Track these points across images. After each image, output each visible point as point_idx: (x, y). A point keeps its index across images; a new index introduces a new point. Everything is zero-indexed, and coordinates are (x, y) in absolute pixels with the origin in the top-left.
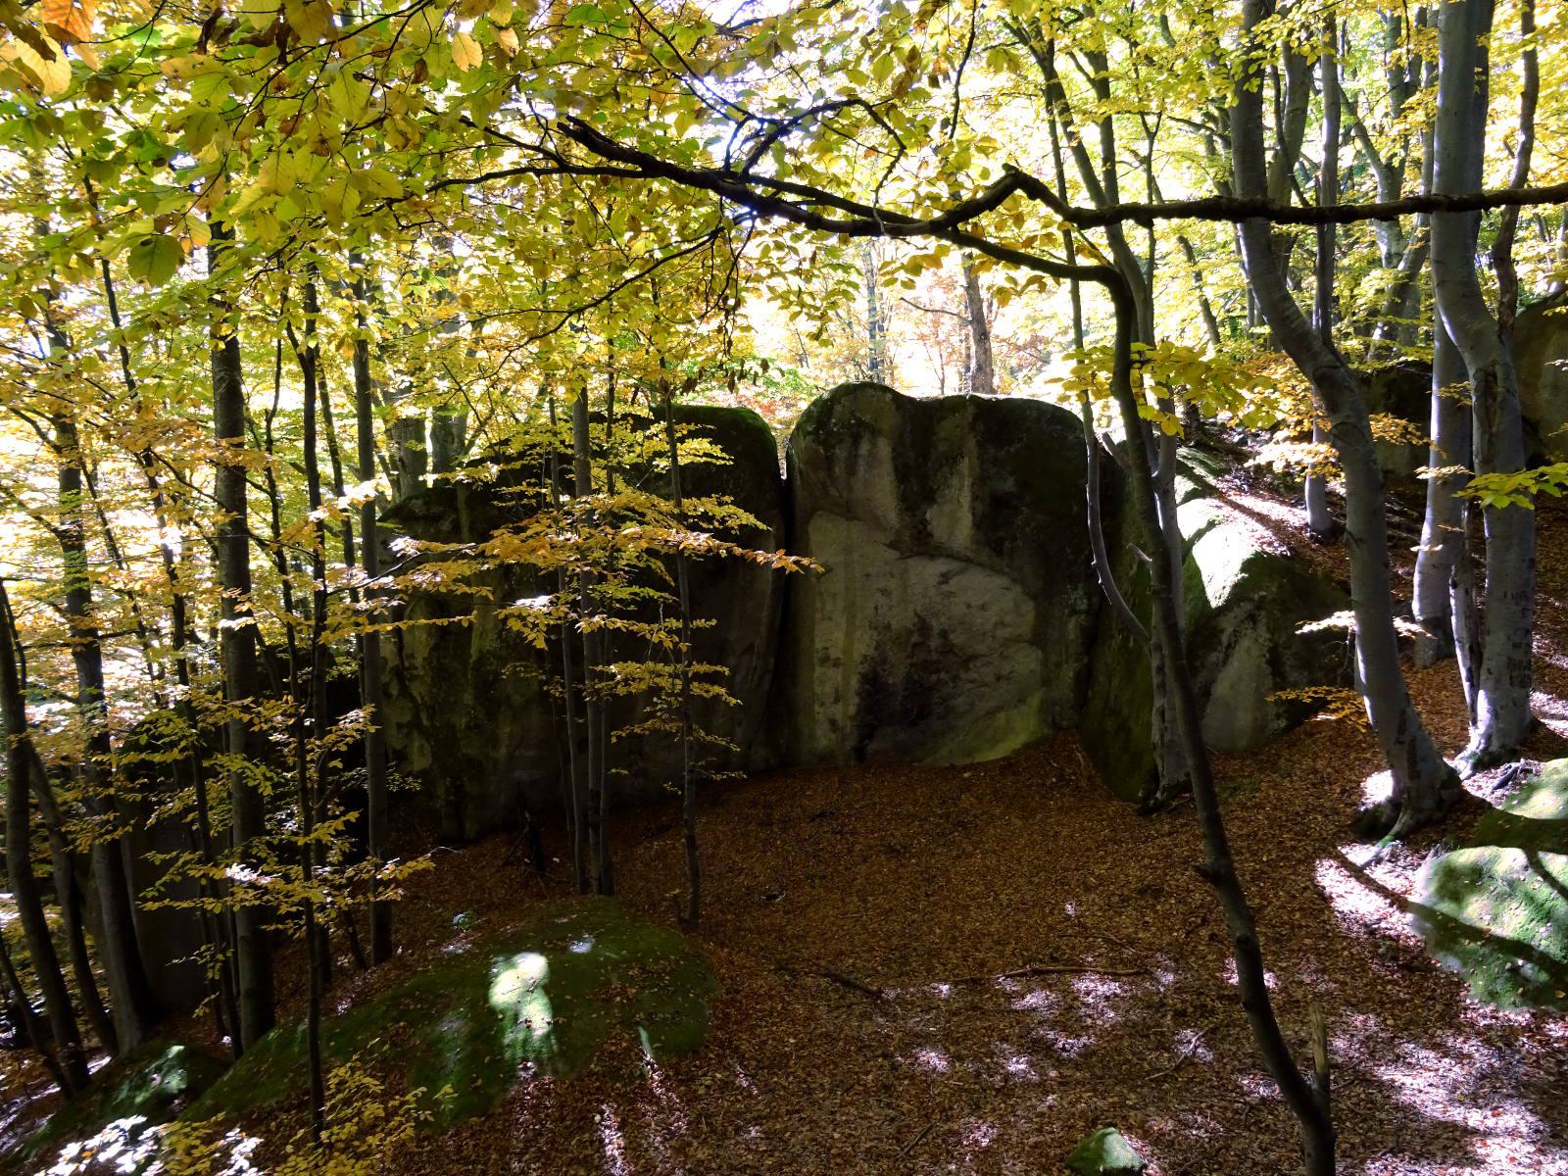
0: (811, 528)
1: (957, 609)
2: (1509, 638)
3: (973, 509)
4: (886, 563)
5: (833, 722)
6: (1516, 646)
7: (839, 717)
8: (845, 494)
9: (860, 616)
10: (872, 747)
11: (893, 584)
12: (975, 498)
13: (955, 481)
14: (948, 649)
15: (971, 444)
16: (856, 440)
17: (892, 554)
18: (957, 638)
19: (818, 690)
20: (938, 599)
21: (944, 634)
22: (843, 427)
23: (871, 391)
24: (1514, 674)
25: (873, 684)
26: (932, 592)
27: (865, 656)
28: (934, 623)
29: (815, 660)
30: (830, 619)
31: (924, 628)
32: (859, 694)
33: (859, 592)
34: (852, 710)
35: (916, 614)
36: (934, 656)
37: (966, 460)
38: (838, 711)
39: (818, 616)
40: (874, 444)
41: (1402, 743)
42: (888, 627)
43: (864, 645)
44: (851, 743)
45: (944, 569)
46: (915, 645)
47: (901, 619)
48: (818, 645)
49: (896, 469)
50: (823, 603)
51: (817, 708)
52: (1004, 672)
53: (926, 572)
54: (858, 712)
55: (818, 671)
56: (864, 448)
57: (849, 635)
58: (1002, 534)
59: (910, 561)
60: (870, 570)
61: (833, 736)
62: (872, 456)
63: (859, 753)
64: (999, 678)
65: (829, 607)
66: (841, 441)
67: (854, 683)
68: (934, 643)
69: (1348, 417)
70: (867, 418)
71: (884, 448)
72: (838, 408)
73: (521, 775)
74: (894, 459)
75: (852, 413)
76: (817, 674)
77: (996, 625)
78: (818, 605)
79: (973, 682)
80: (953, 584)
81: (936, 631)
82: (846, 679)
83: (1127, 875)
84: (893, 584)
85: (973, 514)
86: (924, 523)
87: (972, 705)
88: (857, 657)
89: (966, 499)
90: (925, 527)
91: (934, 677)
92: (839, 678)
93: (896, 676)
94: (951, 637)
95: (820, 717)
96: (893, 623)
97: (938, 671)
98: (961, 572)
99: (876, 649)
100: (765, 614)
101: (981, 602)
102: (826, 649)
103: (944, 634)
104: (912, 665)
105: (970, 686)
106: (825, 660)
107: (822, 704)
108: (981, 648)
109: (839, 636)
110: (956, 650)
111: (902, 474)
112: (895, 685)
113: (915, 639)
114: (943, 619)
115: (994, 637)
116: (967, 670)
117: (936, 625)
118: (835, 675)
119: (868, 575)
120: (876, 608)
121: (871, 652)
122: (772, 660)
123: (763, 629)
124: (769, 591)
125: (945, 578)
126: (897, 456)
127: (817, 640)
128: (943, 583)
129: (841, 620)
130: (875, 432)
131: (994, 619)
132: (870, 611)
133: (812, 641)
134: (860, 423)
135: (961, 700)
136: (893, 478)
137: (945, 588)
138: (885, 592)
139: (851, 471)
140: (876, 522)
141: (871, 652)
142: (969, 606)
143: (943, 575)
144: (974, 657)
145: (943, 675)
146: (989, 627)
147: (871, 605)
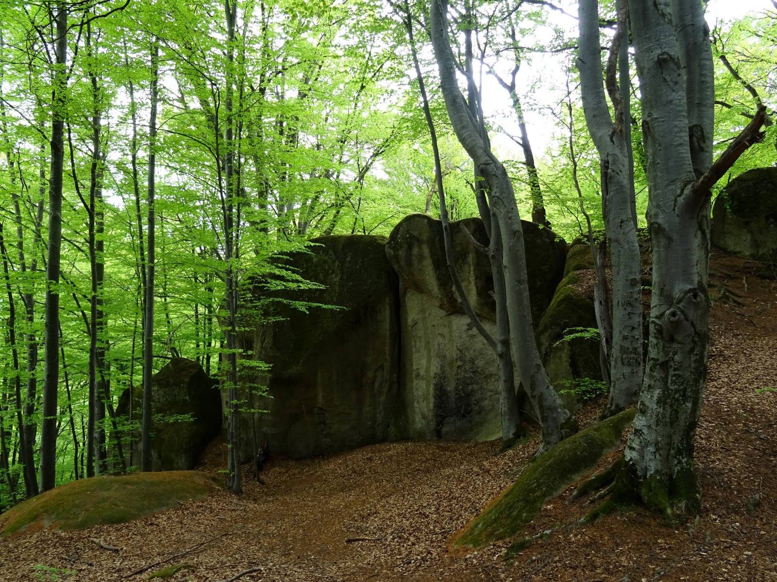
0: (406, 299)
3: (476, 284)
4: (441, 318)
9: (432, 351)
10: (445, 429)
11: (446, 331)
12: (477, 278)
13: (466, 267)
16: (410, 247)
17: (443, 313)
18: (480, 363)
19: (415, 394)
20: (467, 339)
21: (472, 361)
23: (418, 219)
24: (624, 356)
25: (441, 393)
26: (464, 335)
27: (436, 374)
28: (467, 354)
29: (414, 375)
30: (419, 352)
33: (430, 336)
34: (431, 406)
39: (414, 350)
40: (420, 248)
42: (445, 357)
43: (435, 368)
44: (433, 425)
46: (459, 367)
47: (452, 352)
48: (415, 367)
49: (433, 263)
50: (415, 342)
51: (416, 405)
53: (461, 322)
54: (435, 407)
55: (415, 382)
56: (415, 251)
57: (429, 361)
59: (453, 317)
61: (423, 421)
62: (421, 257)
63: (438, 434)
65: (418, 344)
70: (415, 234)
71: (426, 251)
72: (401, 229)
74: (431, 256)
75: (408, 231)
78: (413, 343)
81: (468, 359)
82: (428, 386)
83: (466, 510)
84: (446, 331)
85: (477, 287)
88: (432, 374)
89: (472, 279)
90: (452, 295)
91: (470, 387)
93: (450, 387)
94: (476, 362)
95: (417, 410)
96: (447, 353)
97: (472, 384)
100: (387, 348)
103: (472, 361)
105: (489, 394)
106: (418, 375)
109: (424, 362)
113: (459, 363)
117: (468, 355)
118: (423, 384)
119: (434, 326)
121: (439, 371)
122: (395, 375)
123: (387, 357)
124: (388, 335)
127: (414, 364)
128: (468, 330)
130: (420, 242)
132: (436, 347)
134: (412, 237)
135: (486, 402)
137: (470, 332)
139: (410, 263)
140: (429, 293)
141: (439, 371)
145: (475, 386)
147: (436, 343)
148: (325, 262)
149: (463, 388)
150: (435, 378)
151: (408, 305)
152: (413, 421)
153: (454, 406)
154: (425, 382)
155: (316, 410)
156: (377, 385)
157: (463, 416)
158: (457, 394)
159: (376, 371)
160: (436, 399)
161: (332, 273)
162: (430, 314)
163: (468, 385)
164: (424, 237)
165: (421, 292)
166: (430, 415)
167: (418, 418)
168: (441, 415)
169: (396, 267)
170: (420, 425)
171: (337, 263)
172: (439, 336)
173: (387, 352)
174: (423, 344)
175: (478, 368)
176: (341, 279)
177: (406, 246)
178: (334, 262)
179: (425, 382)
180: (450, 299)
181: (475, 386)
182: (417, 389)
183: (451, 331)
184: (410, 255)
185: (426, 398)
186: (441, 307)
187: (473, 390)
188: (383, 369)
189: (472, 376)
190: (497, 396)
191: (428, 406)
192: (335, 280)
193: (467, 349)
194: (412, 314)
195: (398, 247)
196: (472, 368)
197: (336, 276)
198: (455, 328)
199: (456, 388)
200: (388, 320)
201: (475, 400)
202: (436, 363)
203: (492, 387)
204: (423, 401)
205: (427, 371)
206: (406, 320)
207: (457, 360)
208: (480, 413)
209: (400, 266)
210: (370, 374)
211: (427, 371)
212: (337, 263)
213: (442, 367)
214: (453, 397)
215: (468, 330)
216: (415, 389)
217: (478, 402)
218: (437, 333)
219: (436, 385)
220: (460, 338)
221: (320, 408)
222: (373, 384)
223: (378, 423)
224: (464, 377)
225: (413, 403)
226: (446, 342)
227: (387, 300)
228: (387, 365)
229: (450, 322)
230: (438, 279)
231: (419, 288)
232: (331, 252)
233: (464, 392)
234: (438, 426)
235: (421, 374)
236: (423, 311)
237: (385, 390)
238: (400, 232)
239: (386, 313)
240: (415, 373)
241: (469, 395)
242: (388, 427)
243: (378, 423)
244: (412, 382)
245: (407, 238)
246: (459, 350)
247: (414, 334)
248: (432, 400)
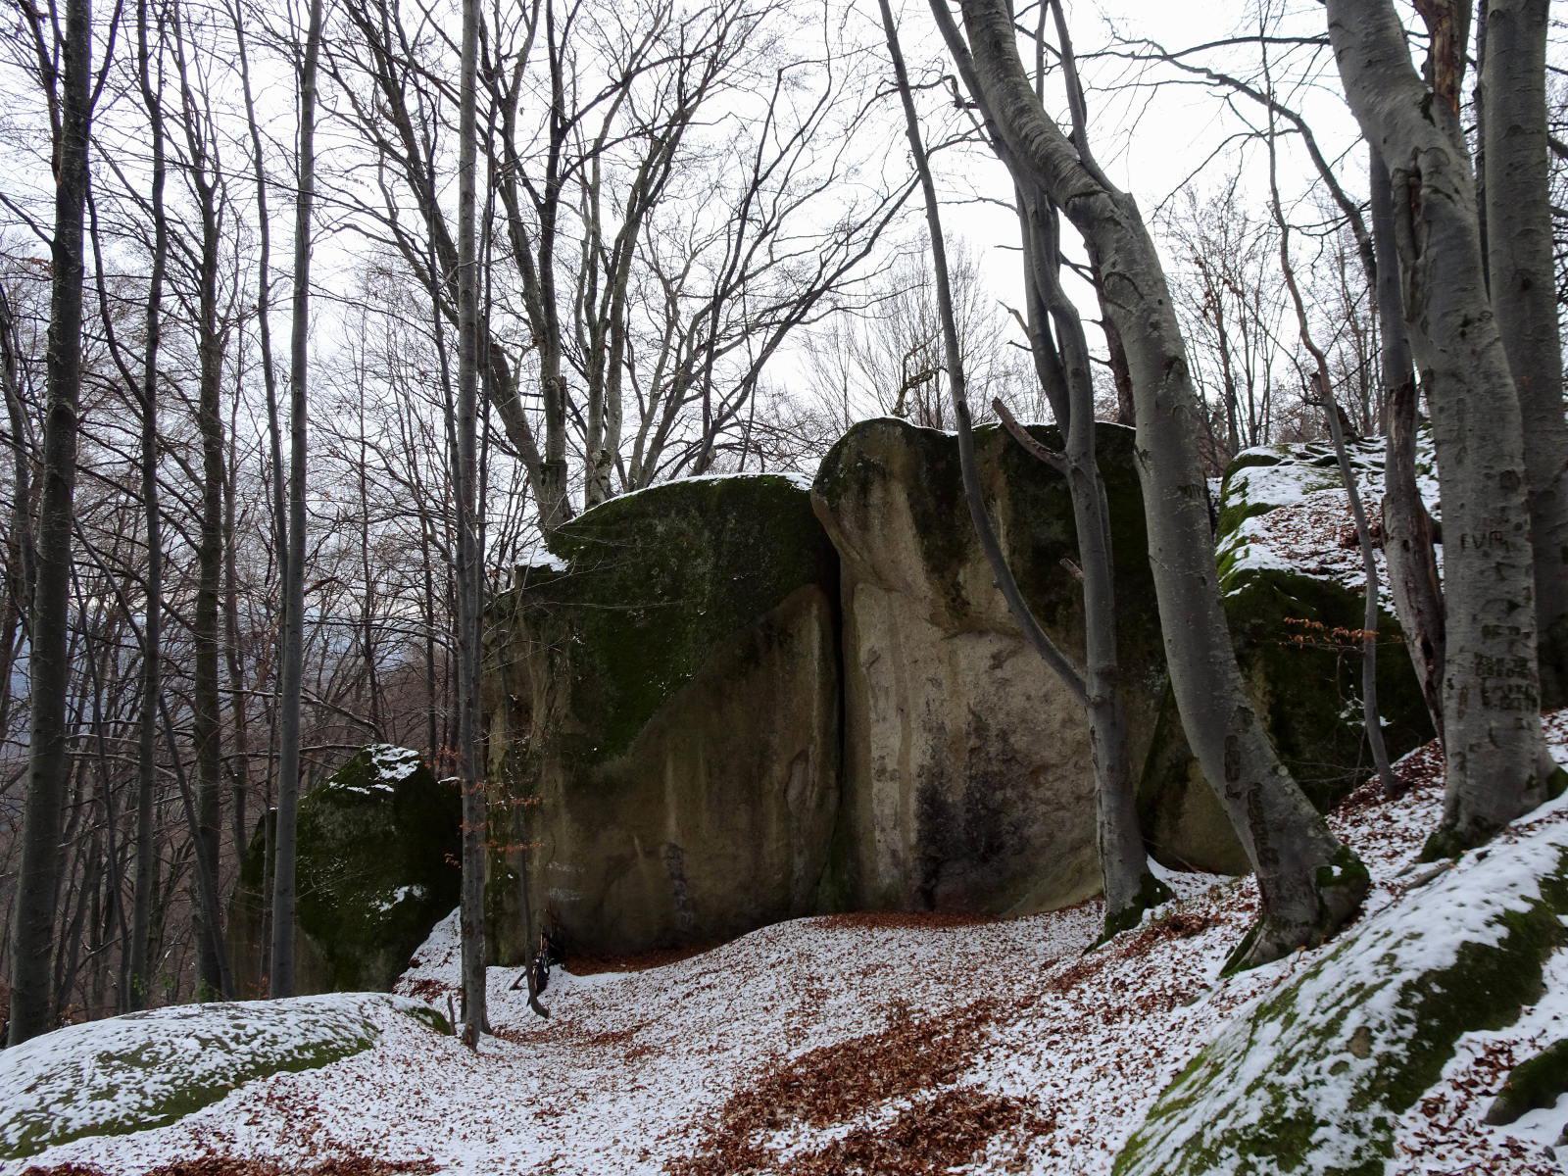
0: (856, 606)
1: (1017, 702)
2: (1474, 618)
4: (933, 645)
5: (894, 853)
6: (1489, 632)
7: (900, 846)
8: (866, 555)
9: (913, 716)
14: (1010, 758)
15: (1001, 481)
16: (865, 489)
17: (936, 633)
18: (1019, 741)
19: (877, 812)
20: (993, 690)
21: (1003, 736)
22: (849, 471)
25: (933, 805)
26: (984, 679)
27: (922, 767)
28: (990, 721)
30: (884, 719)
31: (980, 728)
32: (918, 817)
34: (913, 837)
35: (970, 709)
36: (995, 767)
37: (999, 502)
38: (895, 838)
39: (873, 716)
40: (887, 490)
41: (1237, 796)
42: (941, 728)
44: (917, 879)
45: (994, 648)
46: (973, 751)
47: (956, 718)
48: (875, 754)
50: (877, 701)
51: (878, 835)
52: (1084, 791)
53: (976, 653)
54: (920, 840)
55: (876, 786)
56: (876, 495)
57: (906, 739)
58: (1053, 597)
59: (956, 641)
60: (919, 655)
61: (895, 872)
62: (888, 505)
64: (1079, 798)
65: (882, 704)
66: (846, 489)
67: (913, 804)
68: (994, 748)
69: (1114, 265)
70: (875, 459)
71: (900, 498)
72: (845, 451)
73: (558, 894)
75: (859, 454)
76: (875, 790)
77: (1064, 724)
78: (871, 702)
79: (1046, 802)
80: (1007, 671)
86: (957, 587)
87: (1051, 836)
88: (914, 768)
90: (958, 592)
91: (999, 795)
92: (897, 796)
94: (1012, 740)
95: (881, 847)
96: (949, 726)
97: (1002, 787)
98: (1013, 653)
99: (933, 758)
101: (1041, 694)
102: (883, 758)
103: (1003, 736)
104: (971, 777)
105: (1042, 808)
106: (882, 771)
107: (883, 830)
108: (1050, 755)
109: (895, 742)
110: (1019, 757)
111: (924, 527)
112: (954, 805)
113: (973, 742)
114: (1001, 716)
115: (1063, 741)
116: (1038, 785)
120: (928, 704)
121: (927, 761)
122: (832, 774)
123: (816, 733)
125: (998, 661)
126: (914, 503)
127: (874, 746)
128: (994, 667)
129: (895, 719)
130: (885, 476)
131: (1060, 716)
132: (923, 707)
133: (869, 750)
134: (868, 466)
135: (1035, 828)
136: (914, 531)
137: (999, 673)
138: (935, 682)
139: (864, 526)
141: (927, 761)
142: (1029, 698)
143: (994, 657)
144: (1045, 768)
145: (1009, 793)
146: (1056, 725)
147: (922, 701)
148: (681, 533)
149: (984, 796)
150: (919, 776)
151: (859, 618)
152: (873, 871)
153: (964, 837)
154: (896, 785)
155: (663, 849)
156: (793, 793)
157: (984, 859)
158: (968, 811)
159: (791, 764)
160: (922, 822)
161: (696, 556)
162: (907, 638)
163: (995, 790)
164: (897, 465)
165: (889, 590)
166: (911, 859)
167: (883, 864)
168: (935, 859)
169: (833, 534)
170: (888, 881)
171: (707, 534)
172: (929, 687)
173: (815, 722)
174: (893, 701)
175: (1016, 751)
176: (716, 566)
177: (855, 487)
178: (699, 534)
179: (896, 785)
180: (954, 600)
181: (1009, 793)
182: (881, 802)
183: (955, 674)
184: (865, 506)
185: (899, 822)
186: (934, 620)
187: (1005, 801)
188: (807, 760)
189: (1003, 768)
190: (1061, 813)
191: (905, 839)
192: (701, 570)
193: (991, 709)
194: (870, 637)
195: (839, 490)
196: (1004, 752)
197: (705, 562)
198: (963, 664)
199: (969, 794)
200: (816, 652)
201: (1011, 824)
202: (922, 742)
203: (1049, 794)
204: (894, 828)
205: (903, 759)
206: (856, 653)
207: (968, 734)
208: (1020, 852)
209: (842, 532)
210: (778, 770)
211: (903, 759)
212: (707, 534)
213: (935, 752)
214: (962, 816)
215: (994, 667)
216: (875, 801)
217: (1017, 827)
218: (924, 676)
219: (922, 792)
220: (976, 685)
221: (673, 847)
222: (785, 791)
223: (796, 876)
224: (986, 773)
225: (872, 832)
226: (946, 695)
227: (815, 611)
228: (815, 751)
229: (953, 653)
230: (928, 555)
231: (882, 581)
232: (693, 512)
233: (985, 807)
234: (926, 881)
235: (889, 769)
236: (893, 631)
237: (812, 804)
238: (843, 458)
239: (812, 637)
240: (875, 766)
241: (996, 813)
242: (818, 883)
243: (796, 876)
244: (869, 786)
245: (858, 470)
246: (973, 713)
247: (873, 682)
248: (914, 825)
